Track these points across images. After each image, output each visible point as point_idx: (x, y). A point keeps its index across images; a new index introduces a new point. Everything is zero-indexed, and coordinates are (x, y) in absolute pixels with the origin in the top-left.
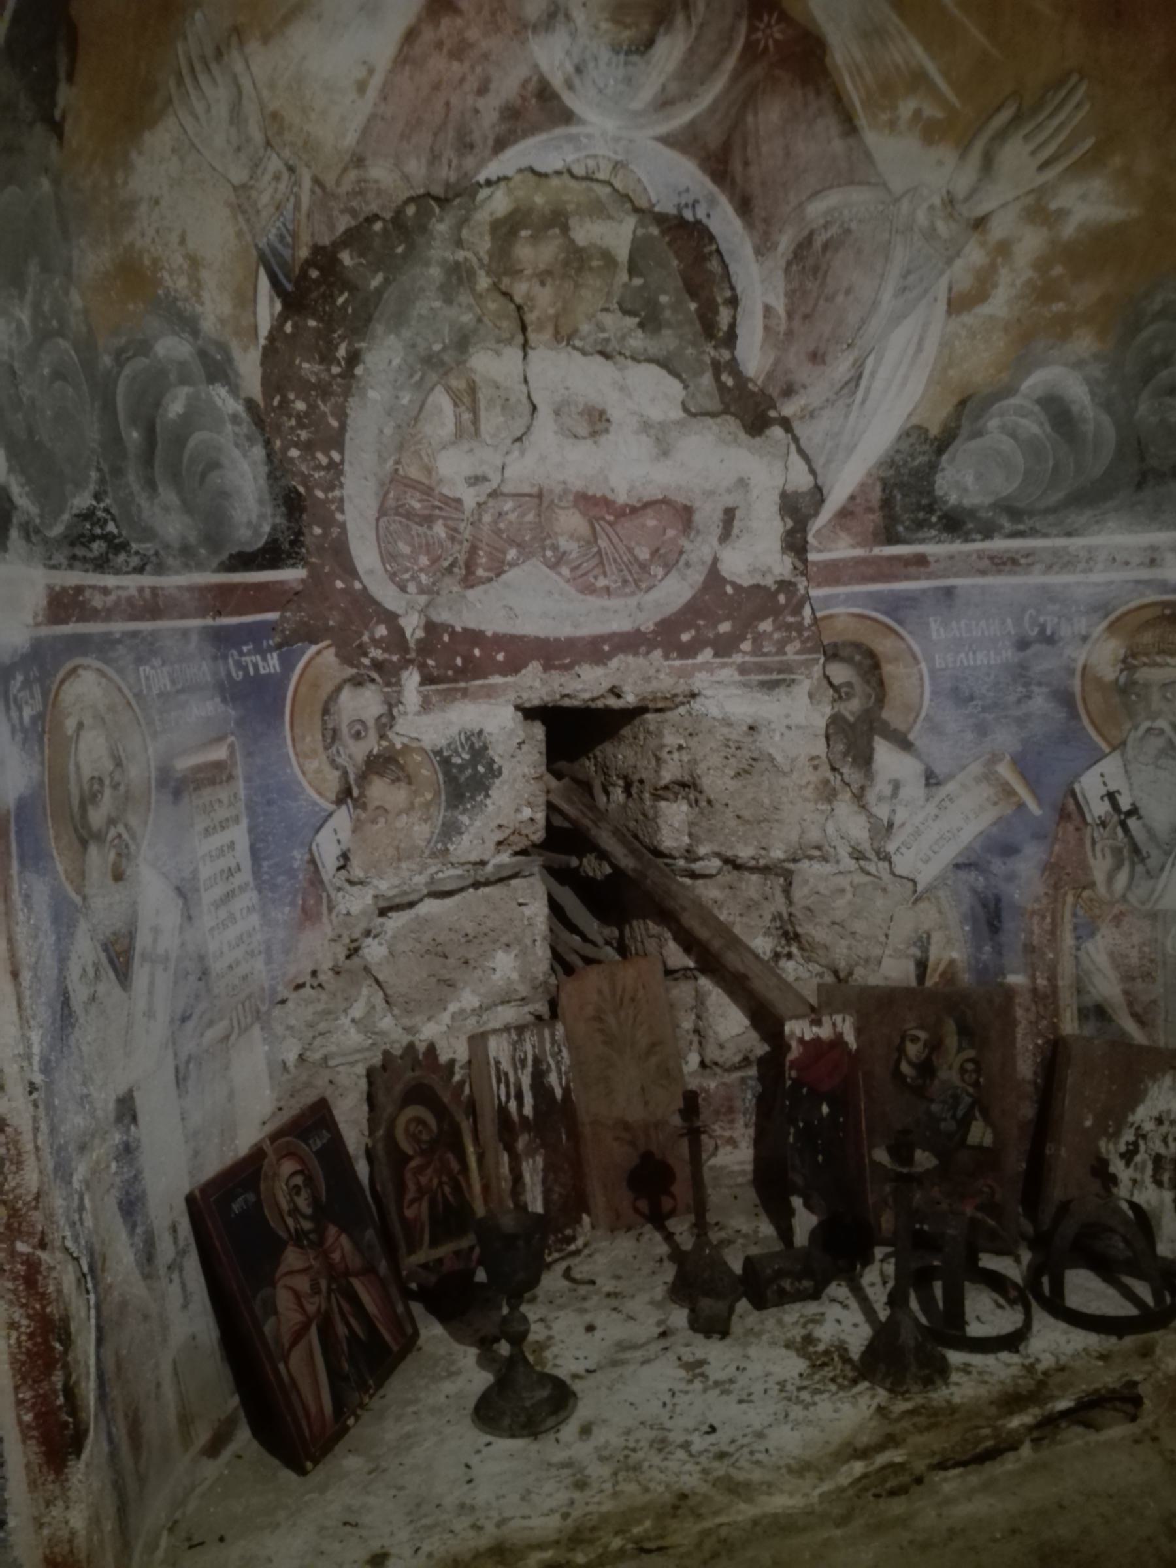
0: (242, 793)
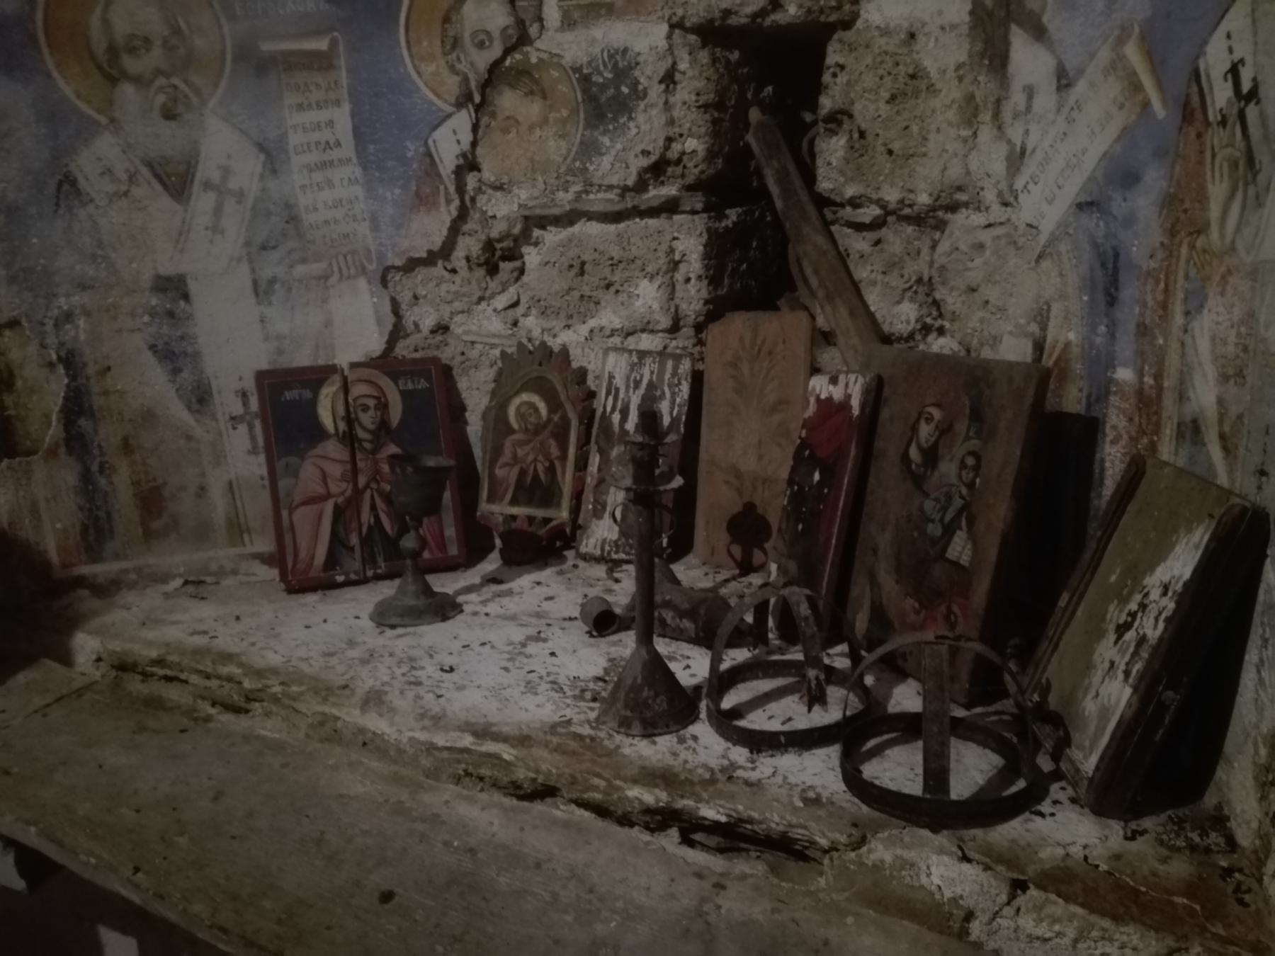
0: (344, 82)
